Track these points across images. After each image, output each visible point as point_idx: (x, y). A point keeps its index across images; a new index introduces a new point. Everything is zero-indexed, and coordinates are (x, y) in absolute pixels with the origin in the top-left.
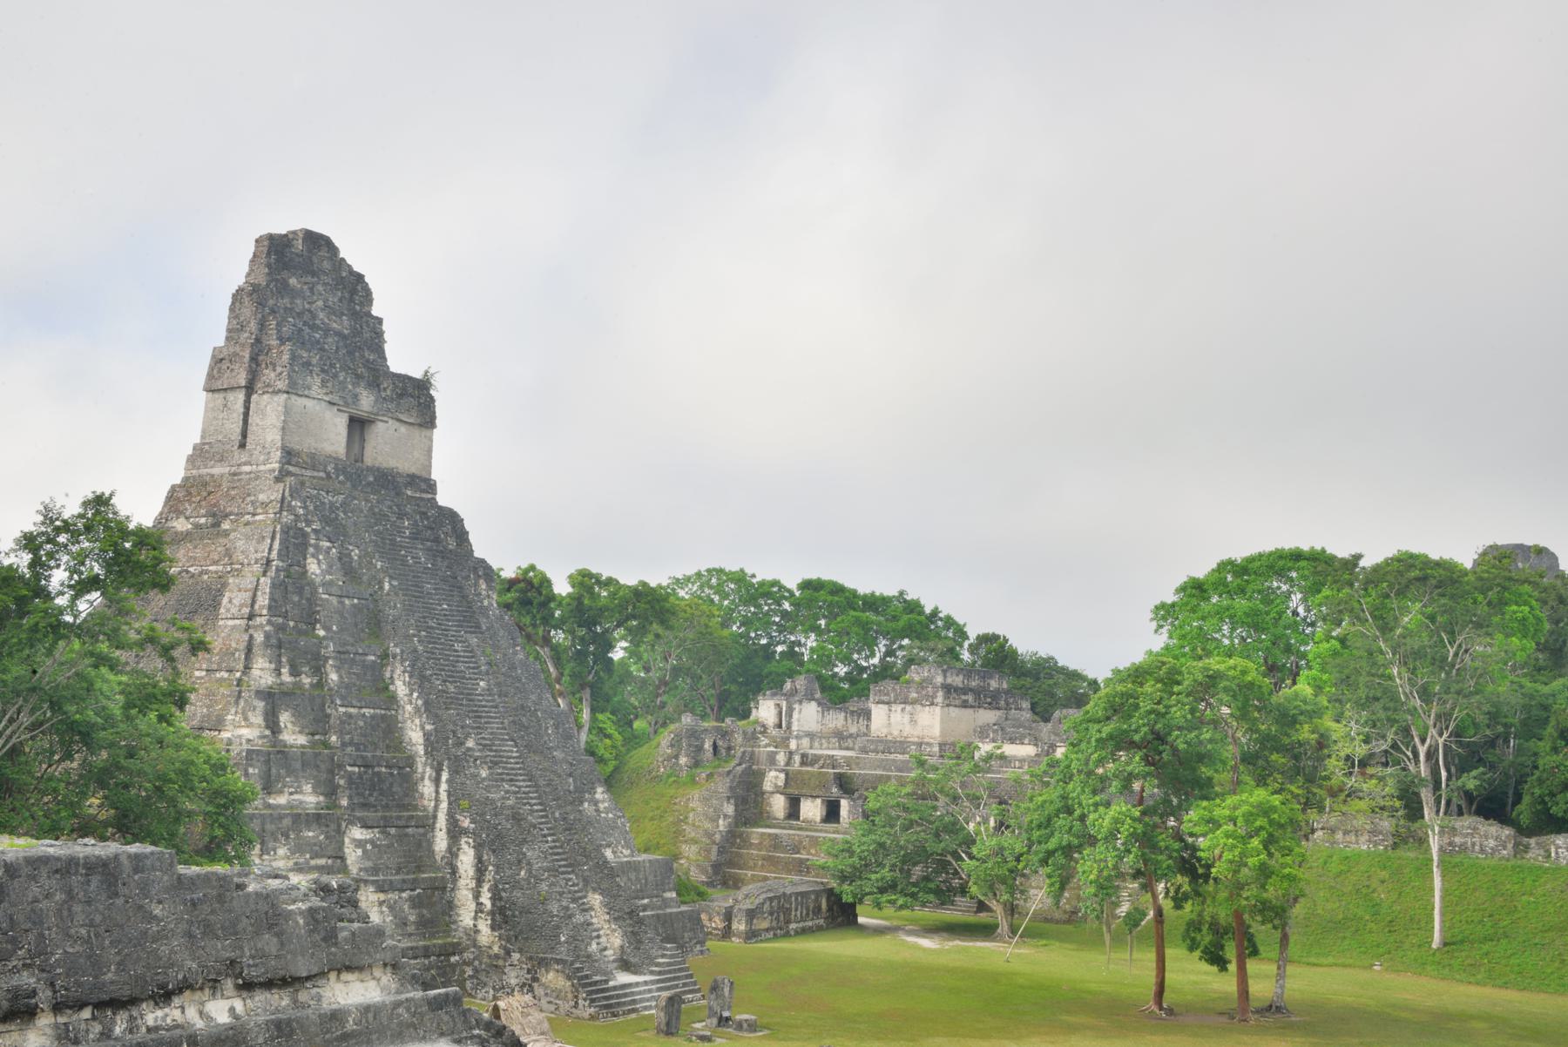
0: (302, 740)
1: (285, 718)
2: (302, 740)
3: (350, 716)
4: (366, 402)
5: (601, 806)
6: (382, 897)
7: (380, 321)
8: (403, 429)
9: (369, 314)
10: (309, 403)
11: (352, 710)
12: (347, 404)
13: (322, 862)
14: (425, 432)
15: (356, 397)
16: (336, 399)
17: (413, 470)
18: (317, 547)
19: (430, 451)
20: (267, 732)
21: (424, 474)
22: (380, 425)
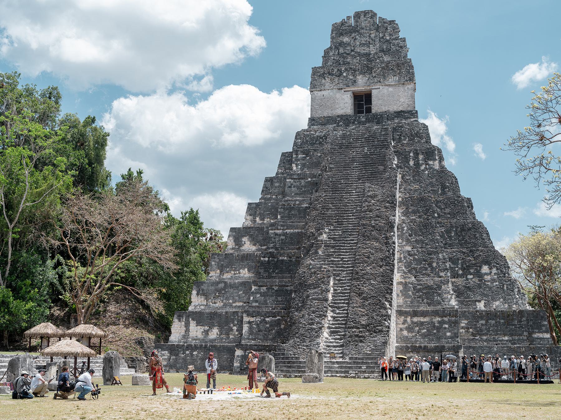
0: (254, 248)
3: (276, 234)
4: (362, 83)
6: (252, 319)
7: (404, 40)
8: (391, 89)
9: (397, 39)
11: (277, 231)
14: (411, 86)
15: (355, 81)
16: (341, 86)
17: (401, 109)
18: (297, 160)
19: (413, 97)
21: (409, 109)
22: (374, 93)
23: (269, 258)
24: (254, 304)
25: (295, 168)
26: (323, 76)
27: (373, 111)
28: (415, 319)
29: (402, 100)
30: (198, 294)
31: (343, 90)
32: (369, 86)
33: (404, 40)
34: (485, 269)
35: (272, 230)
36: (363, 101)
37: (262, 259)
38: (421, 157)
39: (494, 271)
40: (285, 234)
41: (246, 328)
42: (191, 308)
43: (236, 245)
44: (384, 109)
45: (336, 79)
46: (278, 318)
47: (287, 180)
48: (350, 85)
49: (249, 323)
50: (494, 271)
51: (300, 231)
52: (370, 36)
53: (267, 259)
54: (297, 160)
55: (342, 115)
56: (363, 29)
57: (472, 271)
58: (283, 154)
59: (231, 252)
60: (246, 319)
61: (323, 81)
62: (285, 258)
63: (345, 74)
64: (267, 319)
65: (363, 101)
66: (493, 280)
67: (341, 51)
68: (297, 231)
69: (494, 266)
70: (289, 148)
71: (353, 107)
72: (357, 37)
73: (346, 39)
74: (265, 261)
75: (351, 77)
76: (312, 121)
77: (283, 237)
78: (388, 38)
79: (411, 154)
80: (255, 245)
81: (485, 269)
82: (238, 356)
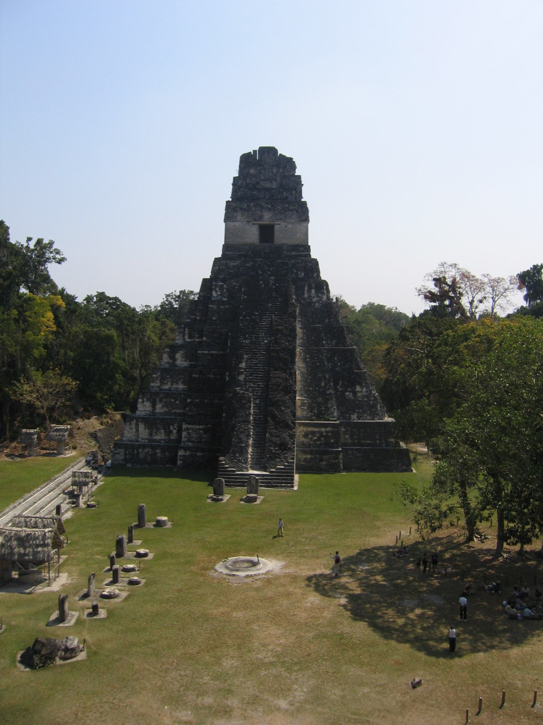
1: (178, 356)
2: (186, 364)
3: (204, 354)
4: (267, 218)
5: (359, 395)
6: (189, 426)
7: (299, 177)
8: (290, 226)
9: (294, 175)
10: (237, 224)
12: (255, 220)
13: (178, 411)
17: (297, 243)
18: (216, 286)
20: (171, 361)
22: (276, 227)
23: (199, 375)
24: (190, 413)
25: (214, 294)
26: (235, 210)
27: (276, 243)
28: (310, 429)
29: (298, 235)
30: (143, 402)
31: (251, 223)
32: (272, 222)
33: (299, 177)
34: (358, 388)
35: (200, 350)
36: (267, 232)
37: (194, 376)
38: (313, 291)
39: (364, 389)
40: (211, 355)
41: (184, 434)
42: (138, 413)
43: (170, 359)
44: (285, 242)
45: (246, 214)
46: (209, 426)
47: (210, 306)
48: (257, 219)
49: (188, 429)
50: (364, 389)
51: (222, 352)
52: (272, 172)
53: (197, 376)
54: (216, 286)
55: (250, 244)
56: (267, 164)
57: (349, 389)
58: (205, 281)
59: (167, 366)
60: (184, 426)
61: (236, 214)
62: (212, 376)
63: (253, 210)
64: (201, 427)
65: (267, 232)
66: (364, 396)
67: (248, 181)
68: (219, 352)
69: (365, 386)
70: (208, 275)
71: (258, 238)
72: (262, 171)
73: (252, 171)
74: (195, 377)
75: (258, 212)
76: (226, 247)
77: (209, 357)
78: (287, 174)
79: (306, 288)
80: (185, 361)
81: (358, 388)
82: (181, 456)
